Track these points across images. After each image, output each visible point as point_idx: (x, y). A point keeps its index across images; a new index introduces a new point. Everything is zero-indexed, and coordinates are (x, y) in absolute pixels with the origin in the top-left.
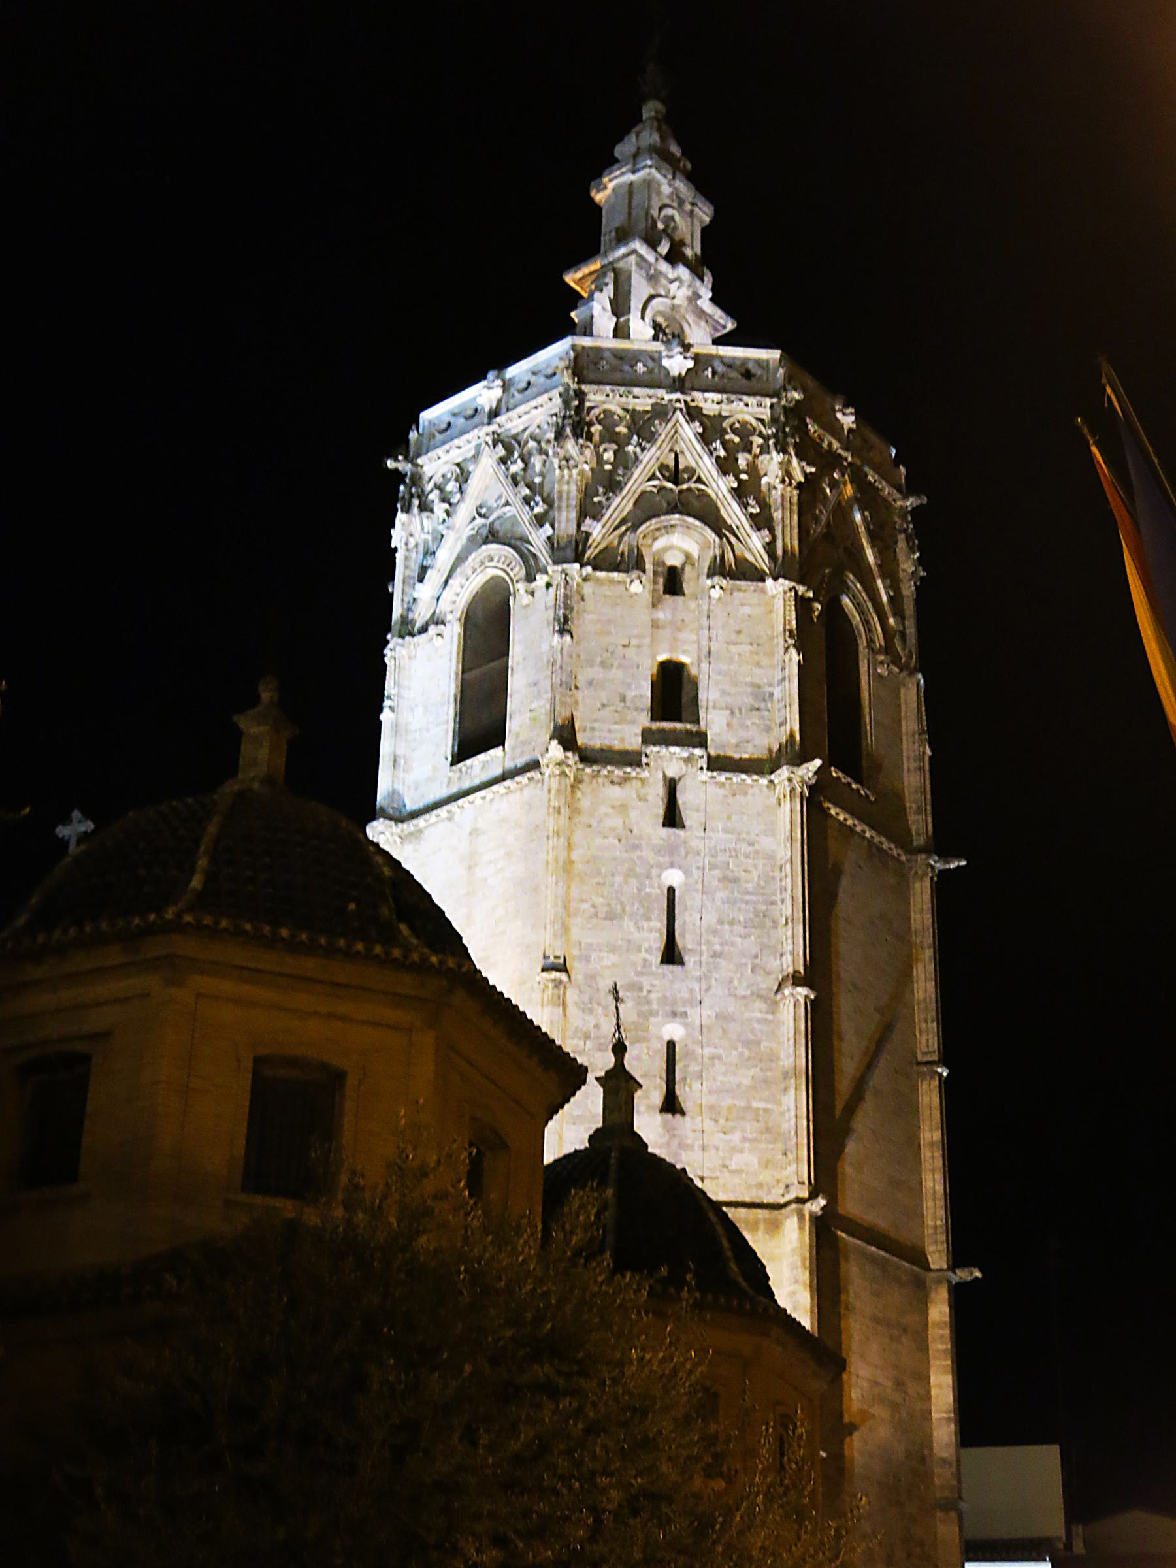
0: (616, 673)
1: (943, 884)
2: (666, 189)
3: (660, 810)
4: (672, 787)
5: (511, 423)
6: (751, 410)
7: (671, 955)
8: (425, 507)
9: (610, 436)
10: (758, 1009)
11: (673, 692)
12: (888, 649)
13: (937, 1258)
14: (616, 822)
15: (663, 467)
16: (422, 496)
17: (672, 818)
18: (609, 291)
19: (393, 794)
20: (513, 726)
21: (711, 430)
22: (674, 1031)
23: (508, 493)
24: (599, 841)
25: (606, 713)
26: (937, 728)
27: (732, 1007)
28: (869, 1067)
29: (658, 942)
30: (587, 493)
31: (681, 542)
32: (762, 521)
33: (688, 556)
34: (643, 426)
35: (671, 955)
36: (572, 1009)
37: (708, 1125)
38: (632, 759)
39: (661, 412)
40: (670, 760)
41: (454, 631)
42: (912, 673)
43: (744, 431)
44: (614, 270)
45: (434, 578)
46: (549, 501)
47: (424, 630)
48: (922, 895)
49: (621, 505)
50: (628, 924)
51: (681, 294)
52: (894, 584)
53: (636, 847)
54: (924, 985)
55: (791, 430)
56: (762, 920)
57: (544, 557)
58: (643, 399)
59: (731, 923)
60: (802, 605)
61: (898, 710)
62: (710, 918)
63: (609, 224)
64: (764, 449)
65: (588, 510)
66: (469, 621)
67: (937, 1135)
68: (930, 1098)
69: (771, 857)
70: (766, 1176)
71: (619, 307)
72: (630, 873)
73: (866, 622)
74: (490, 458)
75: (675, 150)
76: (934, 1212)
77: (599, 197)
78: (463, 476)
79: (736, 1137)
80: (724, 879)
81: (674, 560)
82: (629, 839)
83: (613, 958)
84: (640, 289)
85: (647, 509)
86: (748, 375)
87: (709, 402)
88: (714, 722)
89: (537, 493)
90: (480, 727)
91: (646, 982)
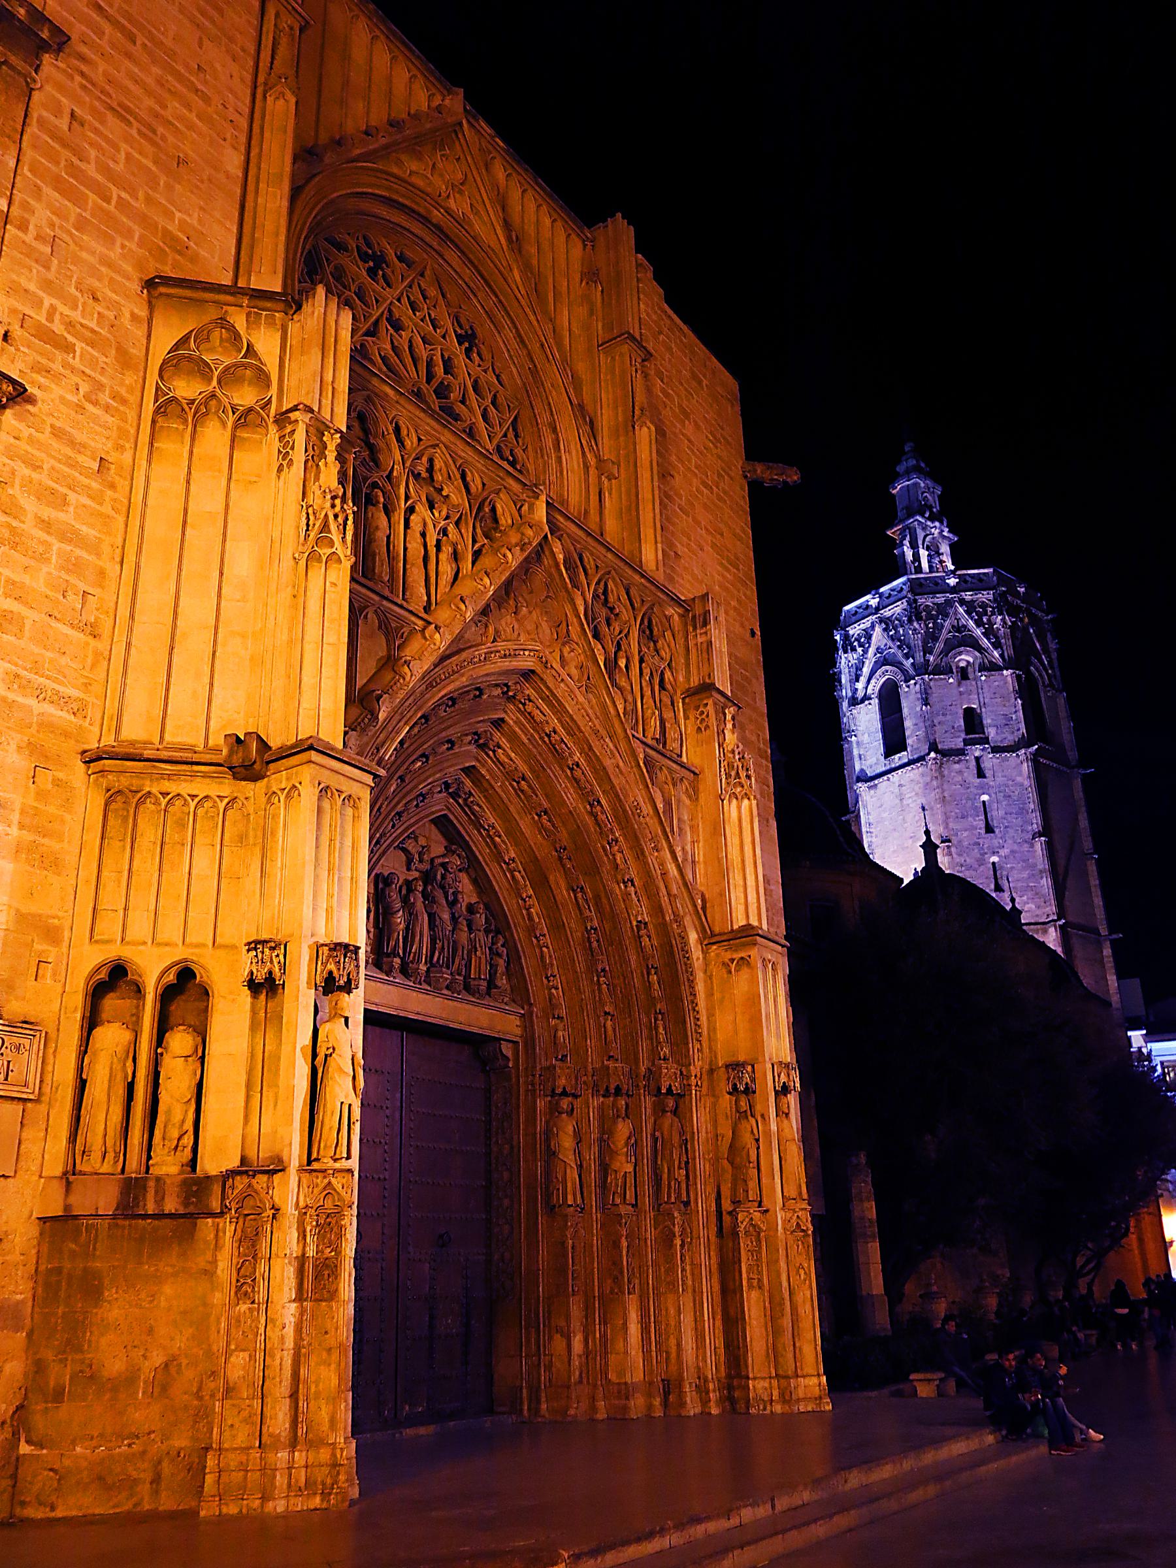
0: (949, 717)
1: (1085, 778)
2: (922, 485)
4: (977, 759)
5: (887, 613)
6: (985, 596)
7: (989, 829)
8: (854, 649)
9: (930, 617)
10: (1026, 847)
11: (973, 721)
12: (1051, 685)
13: (1104, 931)
15: (953, 627)
16: (851, 644)
17: (981, 774)
18: (908, 538)
19: (862, 770)
20: (909, 741)
21: (970, 607)
22: (995, 859)
23: (890, 643)
26: (1073, 715)
27: (1016, 847)
28: (1069, 859)
29: (982, 824)
30: (925, 643)
31: (965, 658)
32: (997, 645)
33: (968, 662)
34: (943, 610)
35: (989, 829)
36: (955, 856)
38: (961, 752)
39: (949, 603)
40: (977, 751)
42: (1061, 692)
43: (984, 606)
44: (909, 528)
45: (863, 680)
46: (909, 647)
47: (862, 701)
48: (1078, 784)
49: (939, 646)
50: (970, 819)
51: (936, 532)
52: (1048, 656)
54: (1084, 822)
55: (1002, 604)
56: (1022, 811)
57: (912, 672)
58: (940, 599)
60: (1018, 677)
61: (1057, 705)
62: (1002, 813)
63: (900, 504)
64: (993, 613)
65: (927, 651)
66: (880, 697)
67: (1097, 882)
68: (1092, 868)
69: (1022, 785)
70: (1038, 912)
71: (914, 546)
72: (968, 799)
73: (1041, 675)
74: (878, 629)
75: (923, 465)
76: (1100, 914)
77: (894, 492)
78: (869, 637)
79: (1025, 898)
81: (963, 664)
82: (964, 784)
83: (965, 834)
84: (920, 534)
85: (952, 646)
86: (981, 580)
87: (968, 596)
88: (991, 732)
89: (903, 644)
90: (894, 741)
91: (981, 841)
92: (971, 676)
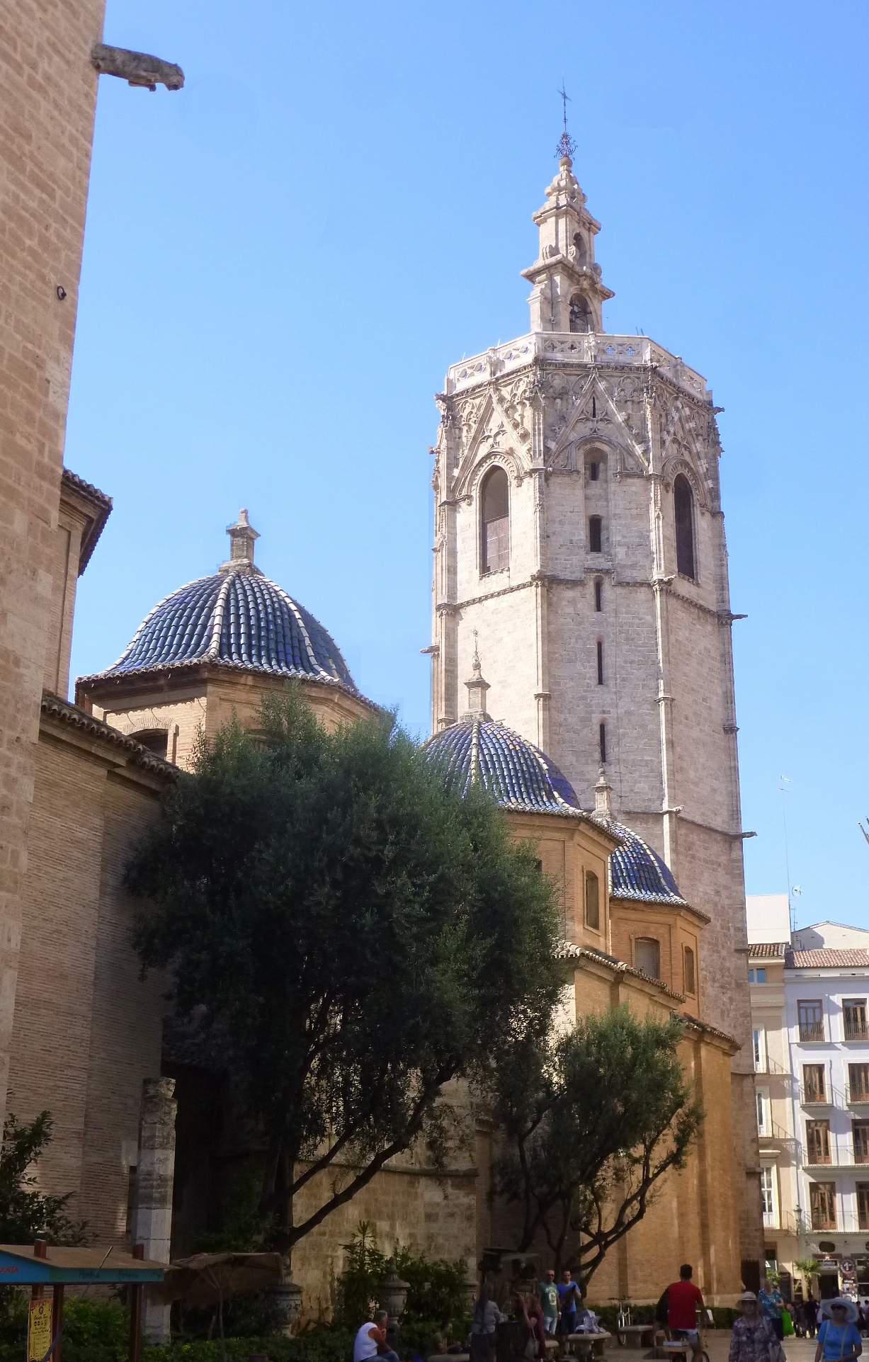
0: (567, 528)
3: (593, 603)
10: (645, 709)
14: (570, 610)
24: (562, 620)
25: (563, 549)
35: (600, 682)
37: (623, 770)
41: (475, 493)
50: (578, 664)
53: (580, 623)
59: (631, 662)
62: (620, 661)
72: (579, 638)
80: (627, 639)
83: (572, 684)
92: (601, 476)
